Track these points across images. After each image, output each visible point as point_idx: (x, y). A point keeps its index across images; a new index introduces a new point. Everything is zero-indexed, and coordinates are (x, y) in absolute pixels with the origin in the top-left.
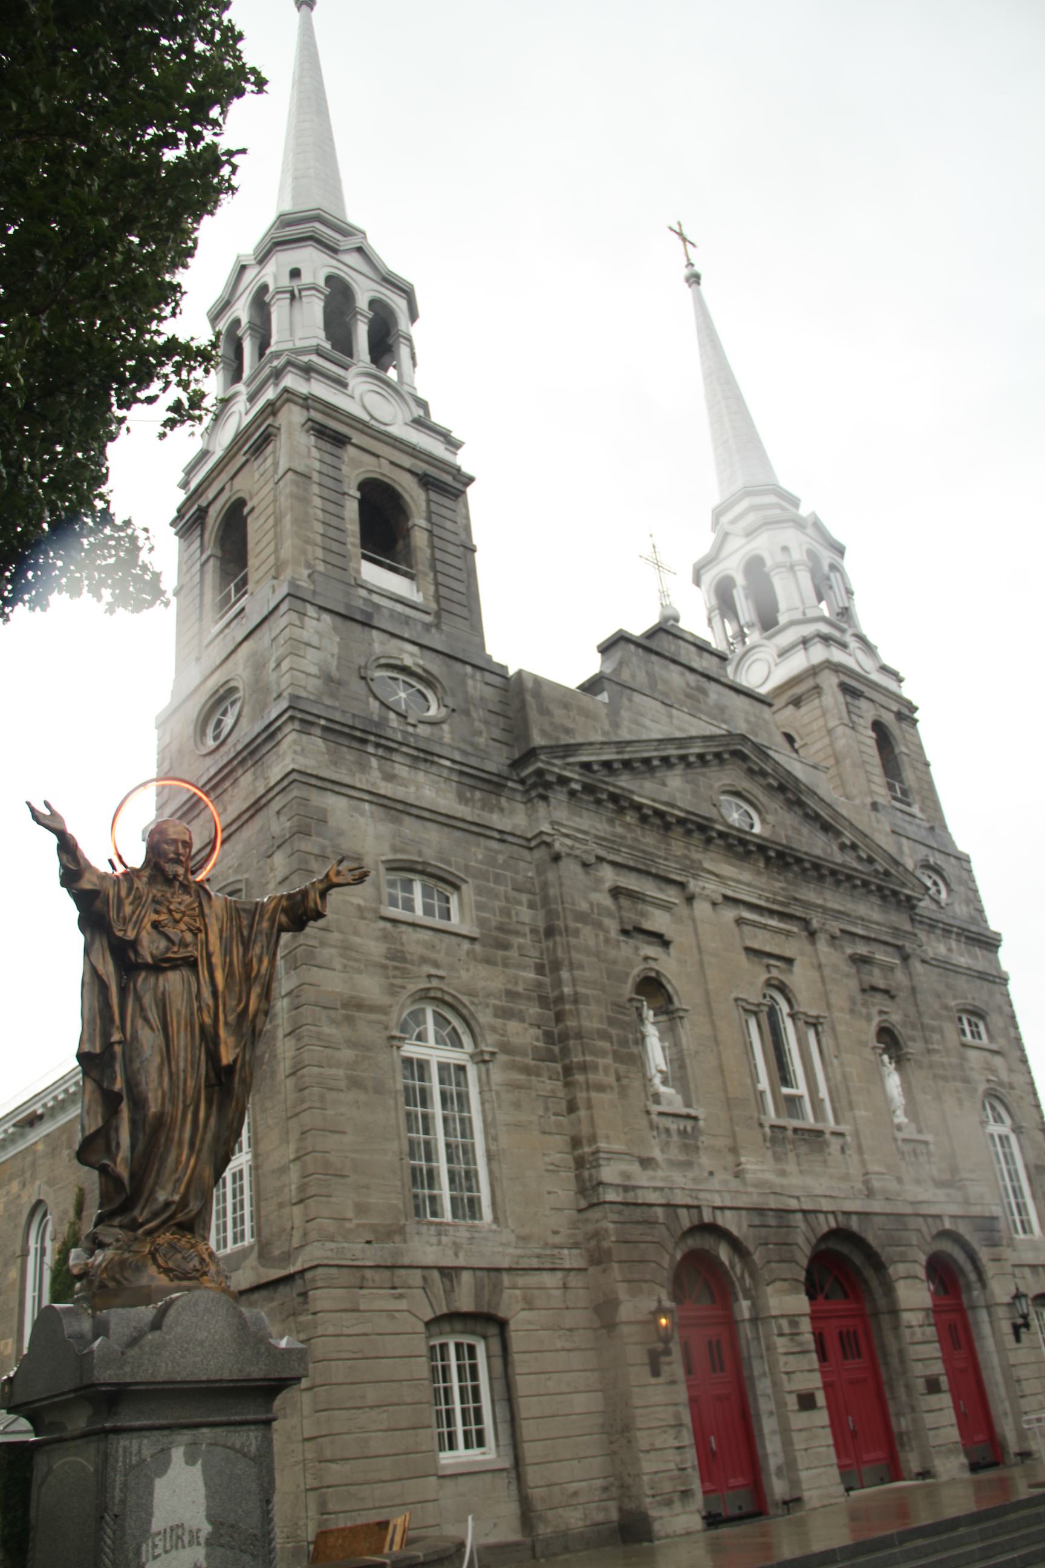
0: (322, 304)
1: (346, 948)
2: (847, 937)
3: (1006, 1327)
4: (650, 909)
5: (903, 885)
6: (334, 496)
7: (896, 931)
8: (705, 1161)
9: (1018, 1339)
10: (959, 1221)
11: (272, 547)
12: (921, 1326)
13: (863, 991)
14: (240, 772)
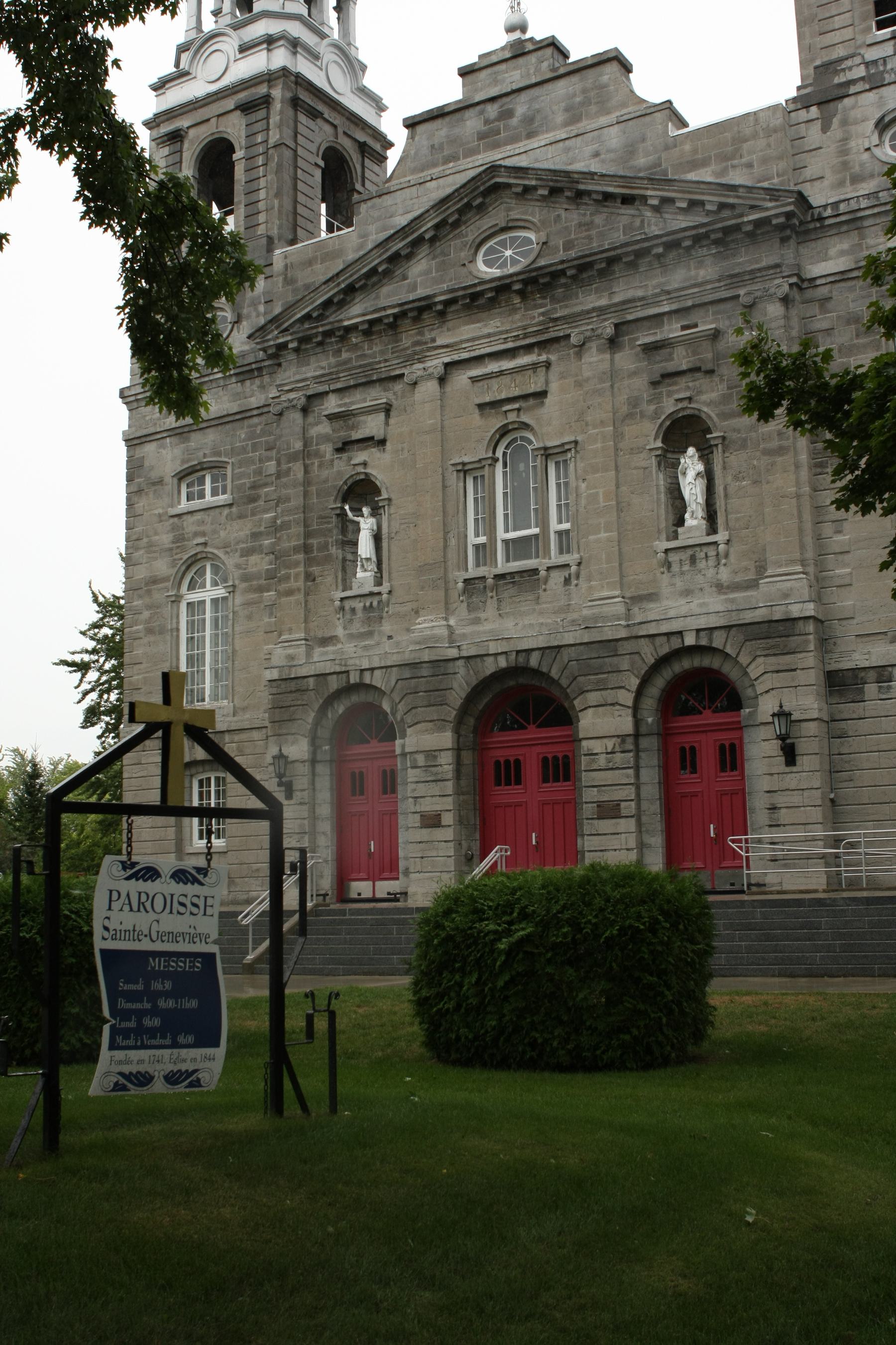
1: (150, 545)
4: (362, 418)
7: (735, 279)
8: (387, 627)
12: (607, 753)
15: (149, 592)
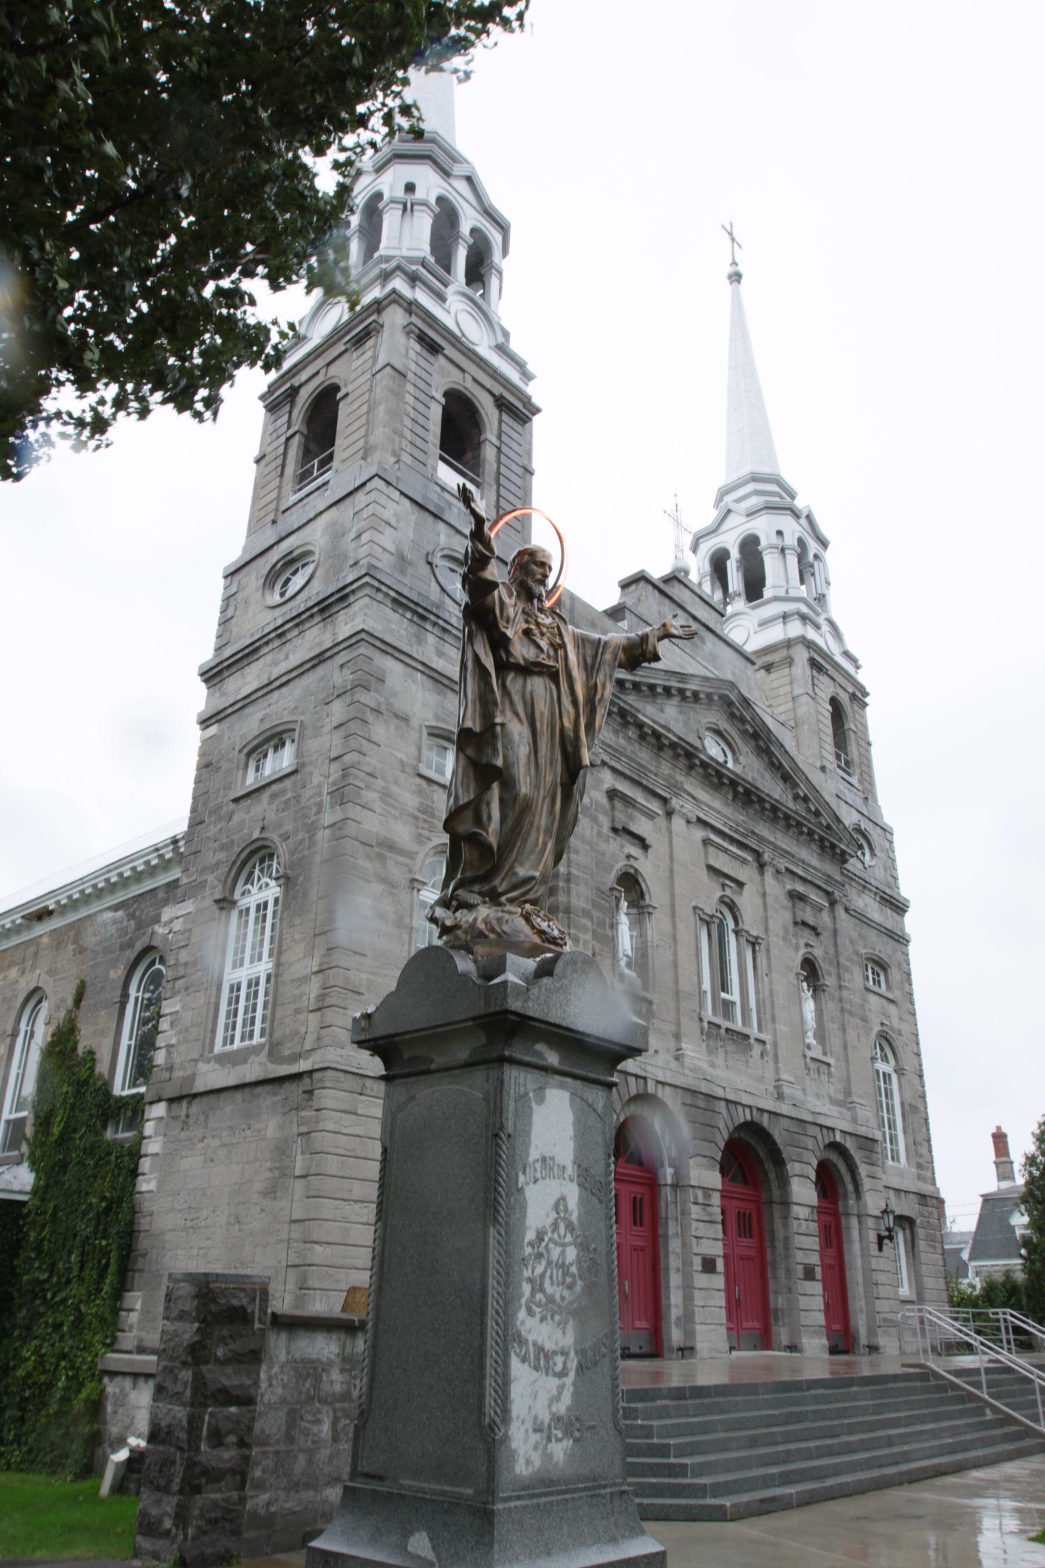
0: (431, 221)
1: (386, 796)
2: (788, 875)
3: (872, 1236)
4: (638, 815)
5: (840, 840)
6: (423, 397)
9: (880, 1249)
10: (848, 1137)
11: (363, 431)
13: (796, 923)
14: (307, 626)
15: (382, 858)
